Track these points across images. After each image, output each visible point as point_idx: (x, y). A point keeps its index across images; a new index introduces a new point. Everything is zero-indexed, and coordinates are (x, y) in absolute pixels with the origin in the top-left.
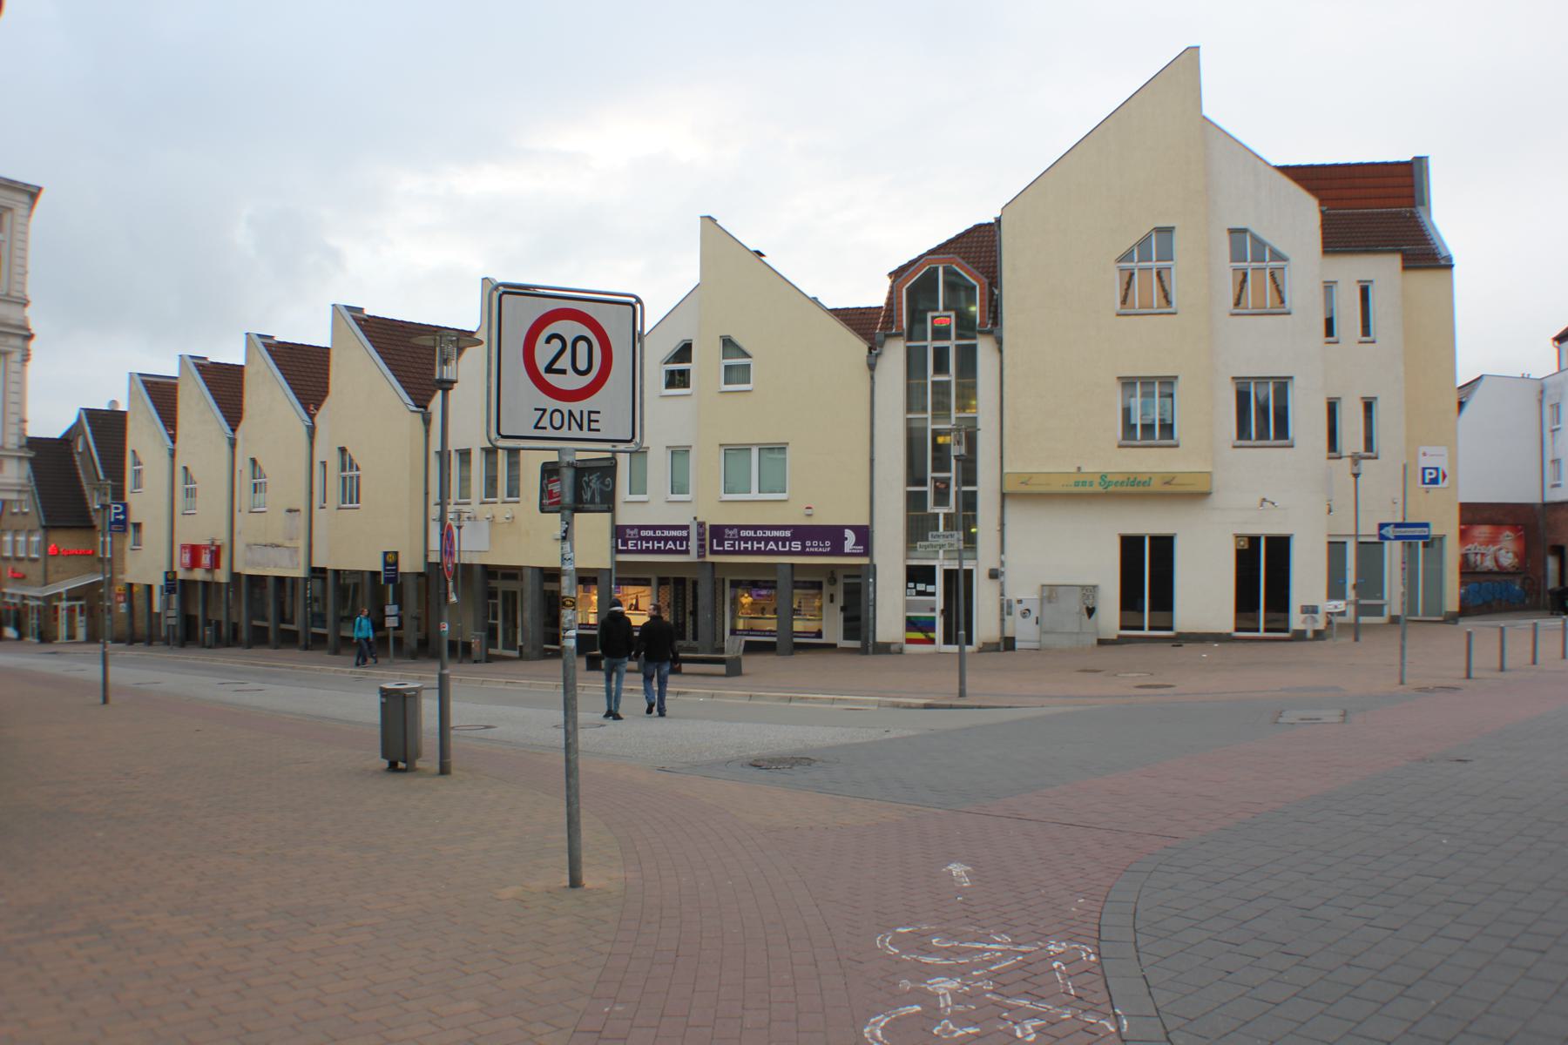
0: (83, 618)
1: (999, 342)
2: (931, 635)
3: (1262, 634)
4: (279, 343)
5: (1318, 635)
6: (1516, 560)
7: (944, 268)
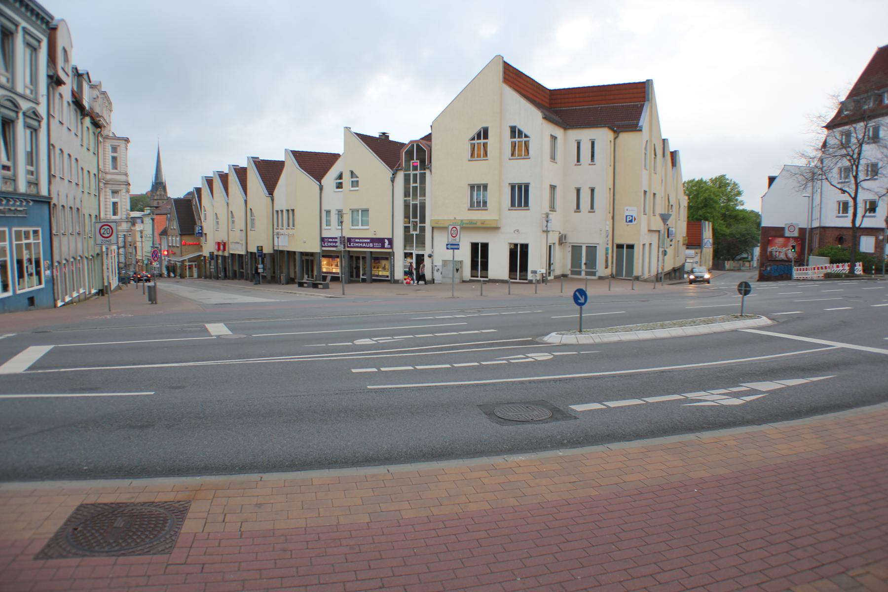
0: (196, 269)
1: (431, 171)
3: (518, 281)
4: (241, 168)
5: (538, 282)
6: (796, 255)
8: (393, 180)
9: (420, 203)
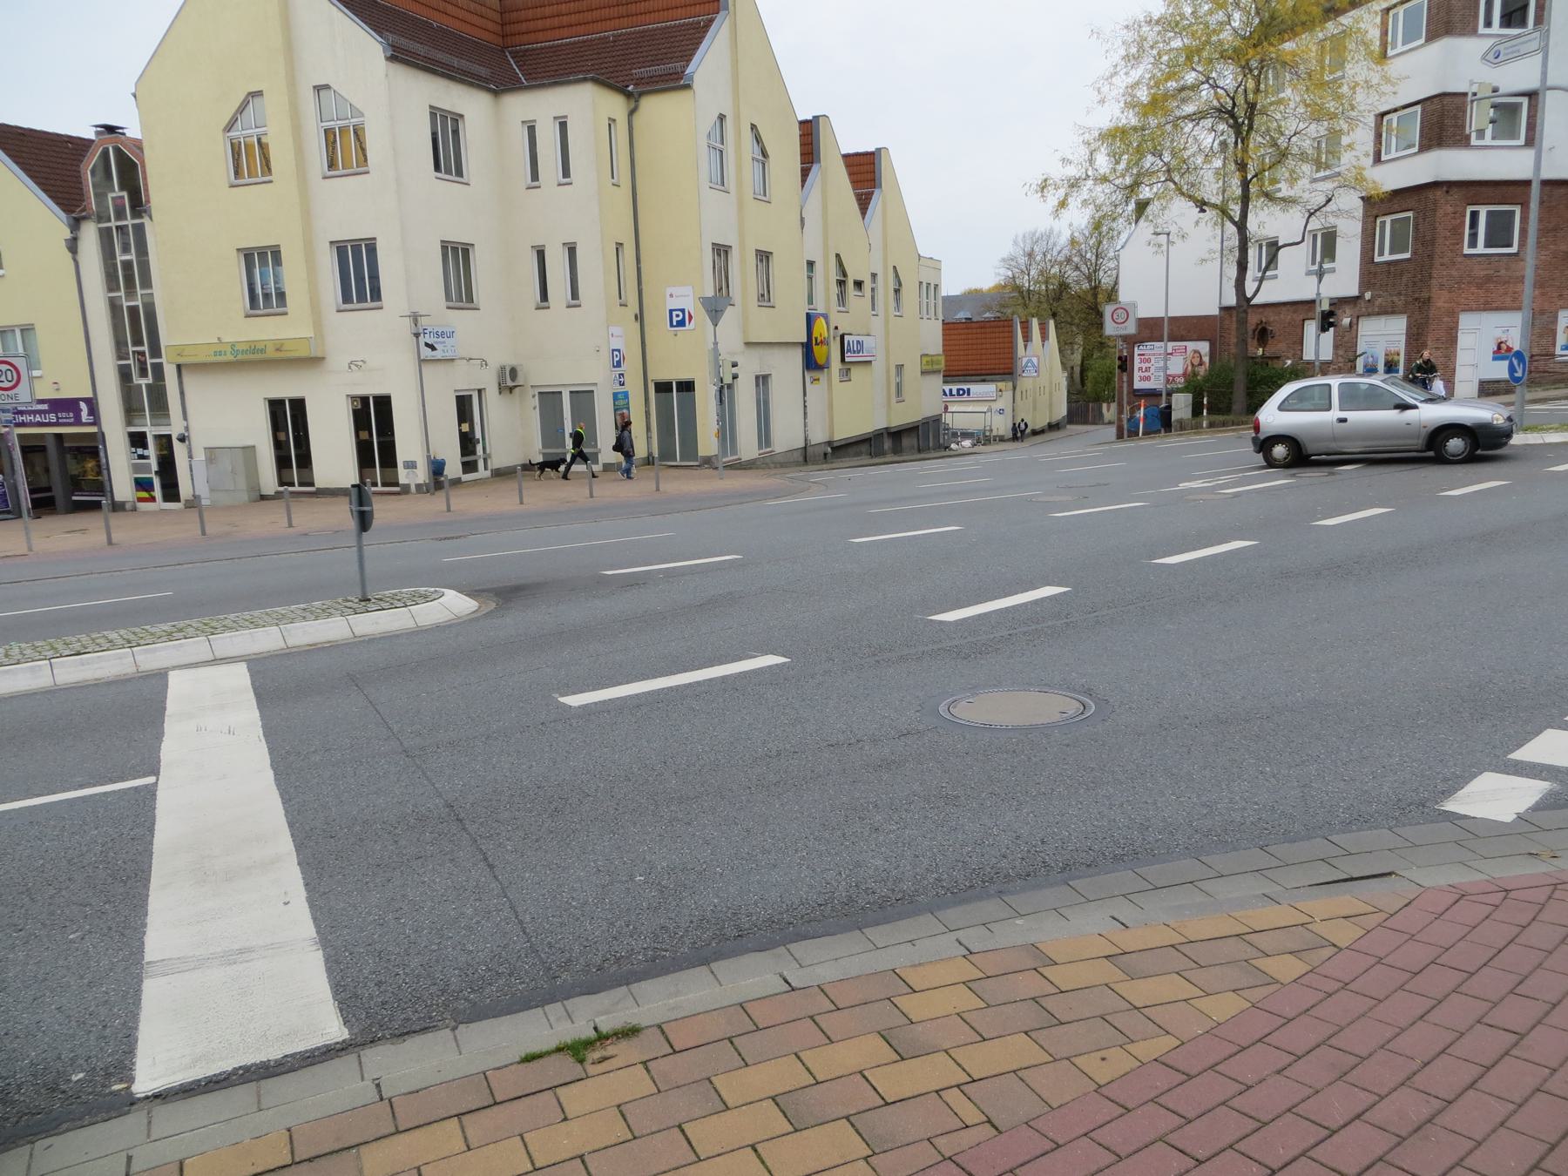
2: (152, 493)
7: (113, 147)
8: (73, 246)
9: (144, 304)
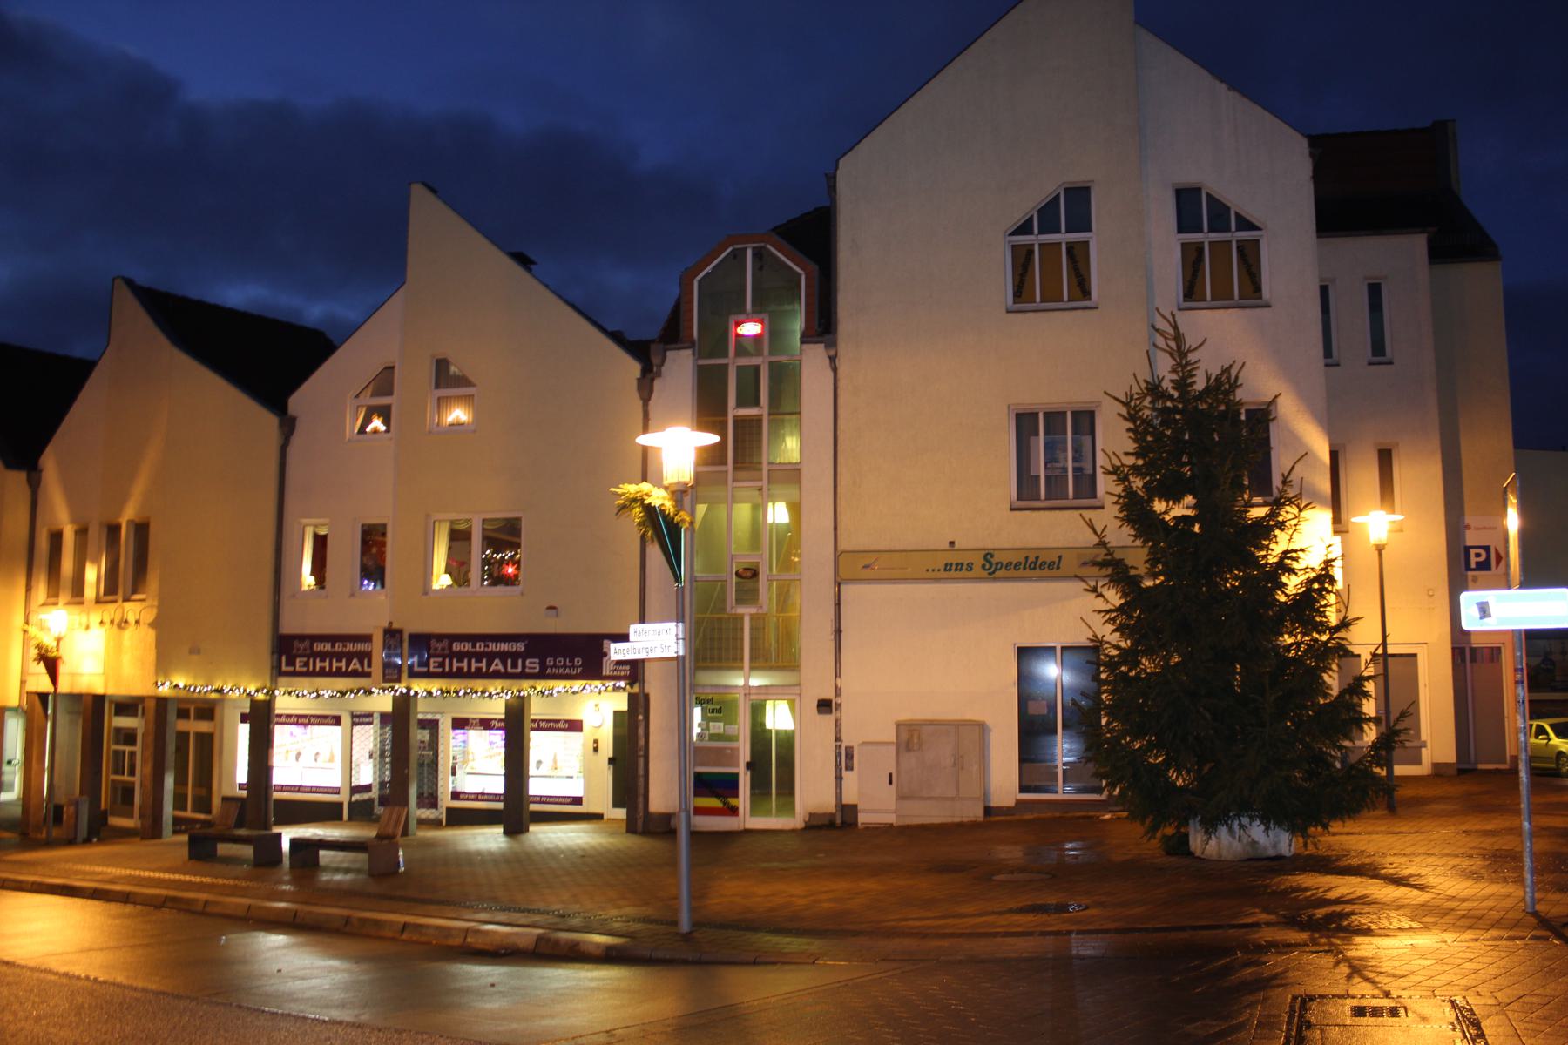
2: (732, 801)
